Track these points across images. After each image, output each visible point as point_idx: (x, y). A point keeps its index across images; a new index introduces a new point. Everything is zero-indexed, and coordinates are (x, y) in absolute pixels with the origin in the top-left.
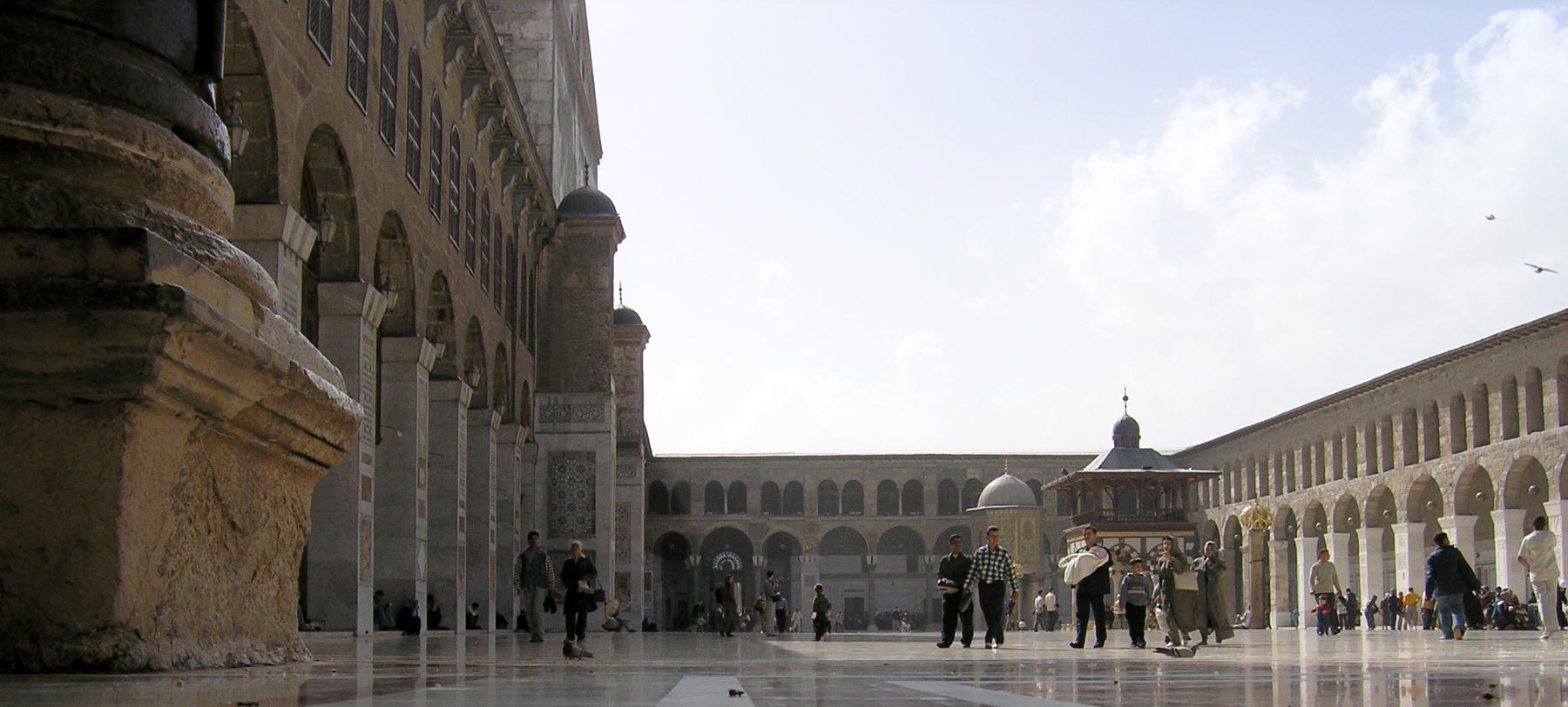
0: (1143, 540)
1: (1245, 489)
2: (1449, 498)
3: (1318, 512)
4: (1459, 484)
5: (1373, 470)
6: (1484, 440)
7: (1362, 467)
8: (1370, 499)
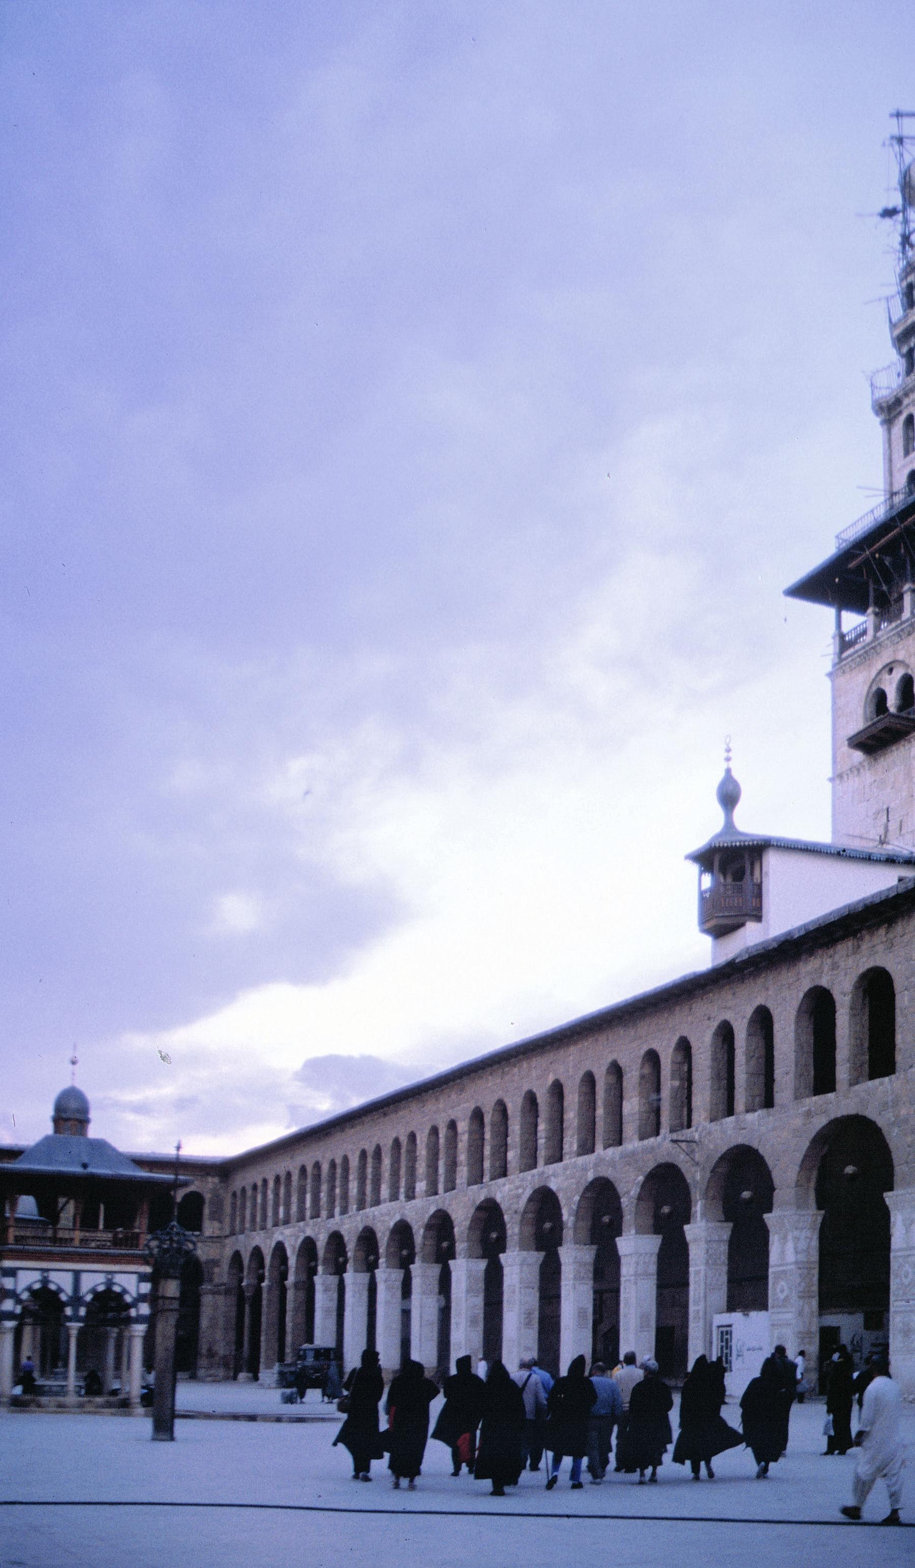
0: (77, 1274)
1: (294, 1208)
2: (513, 1229)
3: (368, 1238)
4: (525, 1212)
5: (433, 1191)
6: (557, 1156)
7: (421, 1186)
8: (428, 1227)
